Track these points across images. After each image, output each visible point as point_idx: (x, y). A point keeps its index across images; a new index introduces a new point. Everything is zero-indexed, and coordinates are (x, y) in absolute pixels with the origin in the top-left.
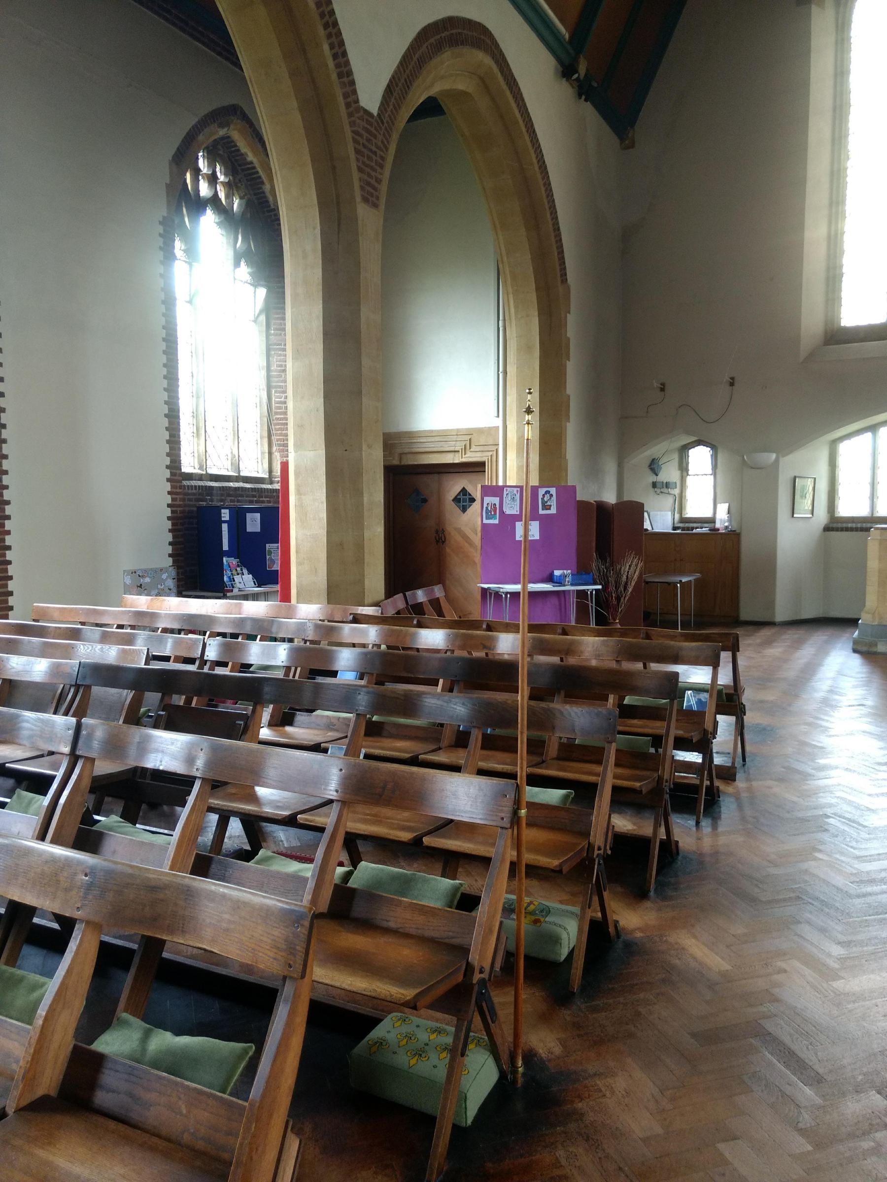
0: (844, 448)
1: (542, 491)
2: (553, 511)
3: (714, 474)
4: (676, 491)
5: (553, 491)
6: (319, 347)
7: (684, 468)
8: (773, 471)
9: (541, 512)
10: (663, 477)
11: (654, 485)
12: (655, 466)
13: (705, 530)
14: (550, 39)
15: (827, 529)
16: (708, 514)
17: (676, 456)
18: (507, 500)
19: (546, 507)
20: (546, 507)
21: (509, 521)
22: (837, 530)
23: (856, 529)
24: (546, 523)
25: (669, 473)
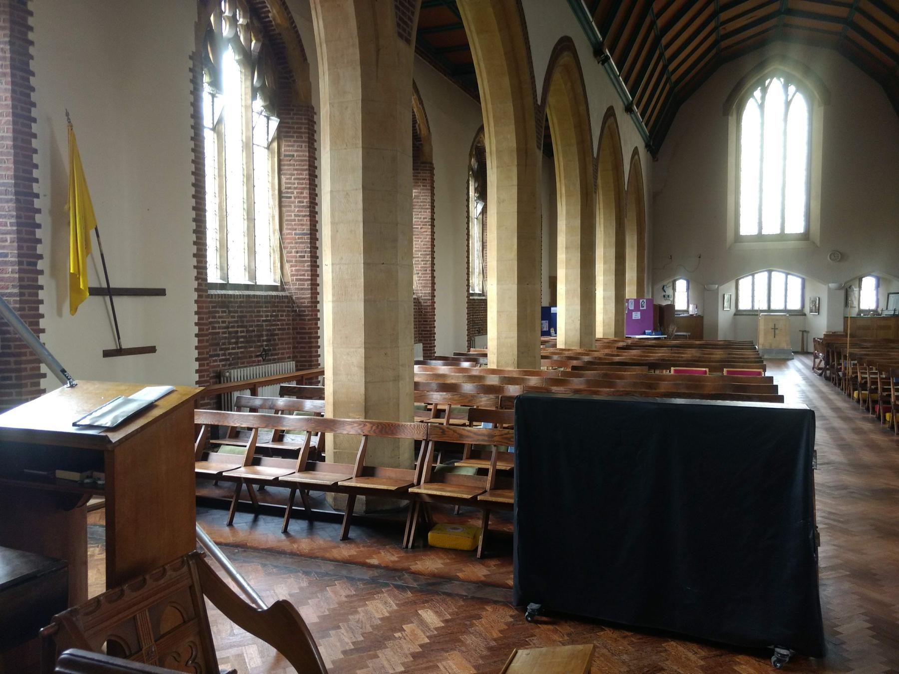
0: (741, 282)
1: (641, 301)
2: (645, 308)
3: (785, 311)
4: (672, 299)
5: (645, 300)
6: (614, 261)
7: (674, 289)
8: (716, 292)
9: (641, 308)
10: (667, 293)
11: (664, 296)
12: (665, 288)
13: (685, 315)
14: (644, 136)
15: (735, 315)
16: (685, 308)
17: (671, 284)
18: (630, 304)
19: (643, 307)
20: (643, 307)
21: (630, 312)
22: (739, 315)
23: (747, 315)
24: (642, 312)
25: (669, 291)
